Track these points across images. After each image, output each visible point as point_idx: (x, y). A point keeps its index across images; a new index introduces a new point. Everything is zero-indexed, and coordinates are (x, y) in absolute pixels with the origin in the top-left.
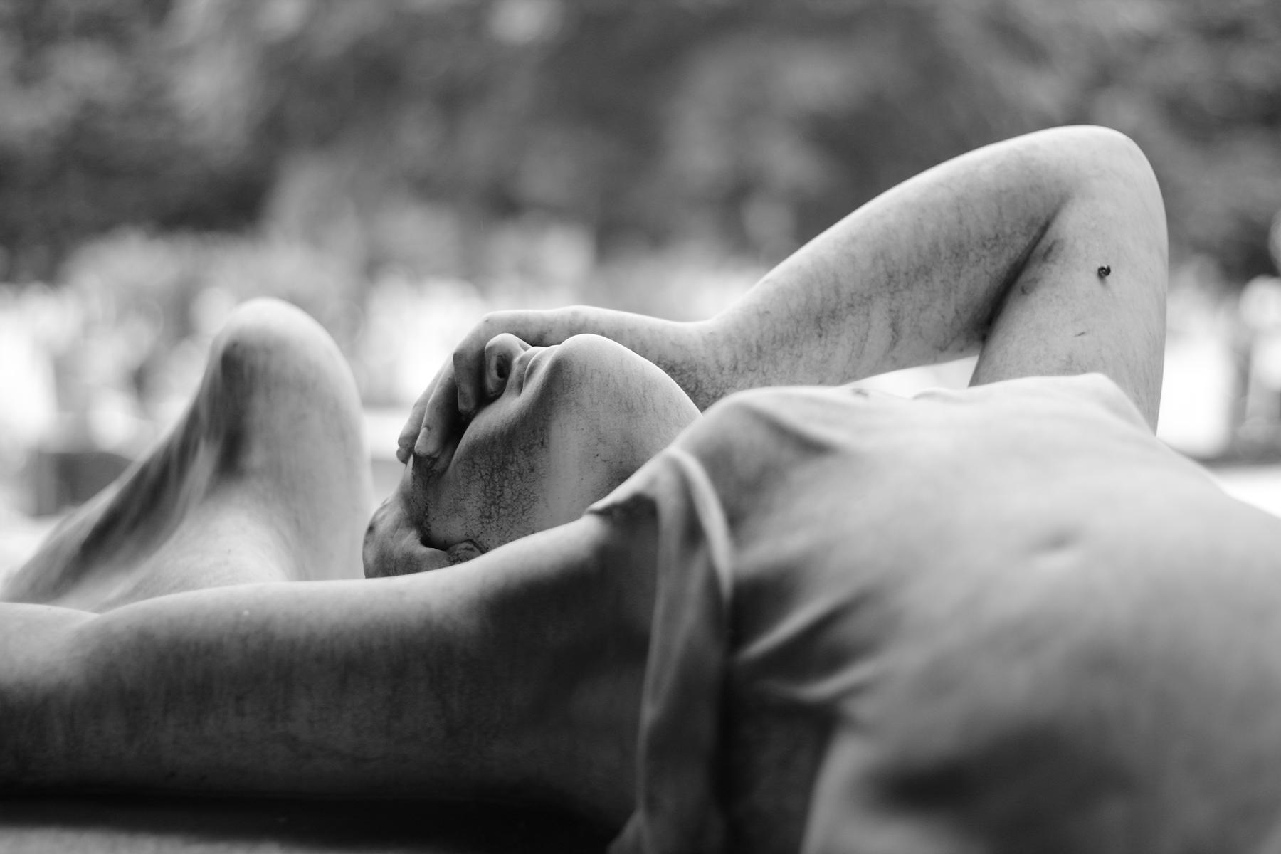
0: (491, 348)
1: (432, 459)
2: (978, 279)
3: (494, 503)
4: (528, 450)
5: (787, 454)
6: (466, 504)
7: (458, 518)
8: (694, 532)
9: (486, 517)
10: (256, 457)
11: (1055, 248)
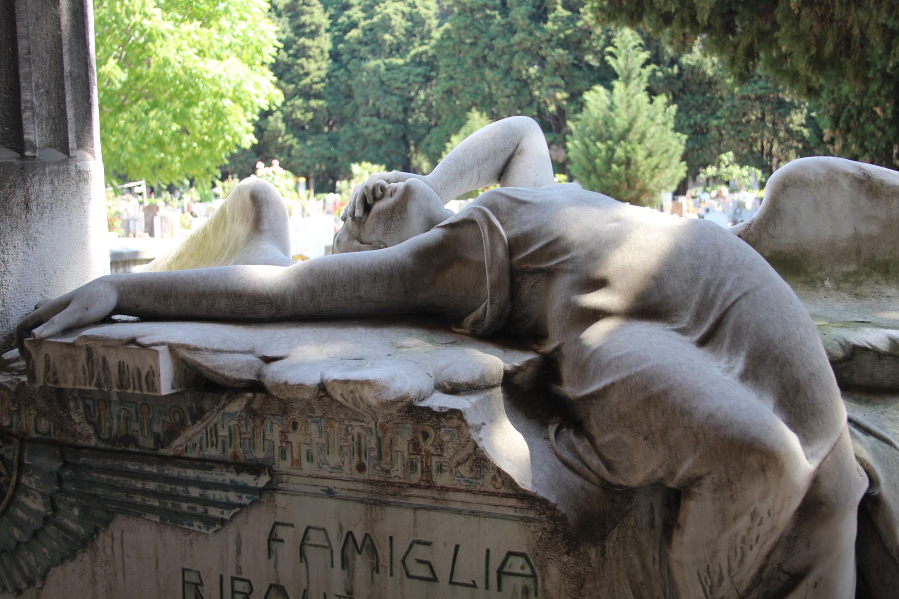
0: (378, 184)
1: (360, 218)
2: (500, 161)
4: (400, 213)
5: (514, 204)
8: (492, 227)
9: (385, 233)
10: (266, 226)
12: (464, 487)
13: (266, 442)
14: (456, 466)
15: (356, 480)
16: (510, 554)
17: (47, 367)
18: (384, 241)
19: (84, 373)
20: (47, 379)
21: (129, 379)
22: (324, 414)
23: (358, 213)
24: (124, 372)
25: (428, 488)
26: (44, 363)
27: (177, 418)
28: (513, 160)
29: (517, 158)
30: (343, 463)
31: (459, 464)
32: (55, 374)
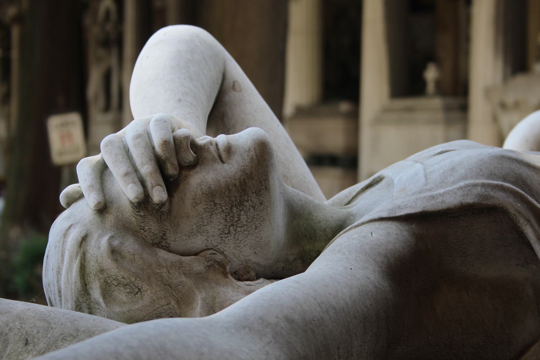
3: (233, 225)
4: (258, 193)
6: (209, 228)
7: (200, 237)
11: (236, 84)
18: (221, 247)
23: (159, 195)
28: (227, 98)
29: (232, 96)
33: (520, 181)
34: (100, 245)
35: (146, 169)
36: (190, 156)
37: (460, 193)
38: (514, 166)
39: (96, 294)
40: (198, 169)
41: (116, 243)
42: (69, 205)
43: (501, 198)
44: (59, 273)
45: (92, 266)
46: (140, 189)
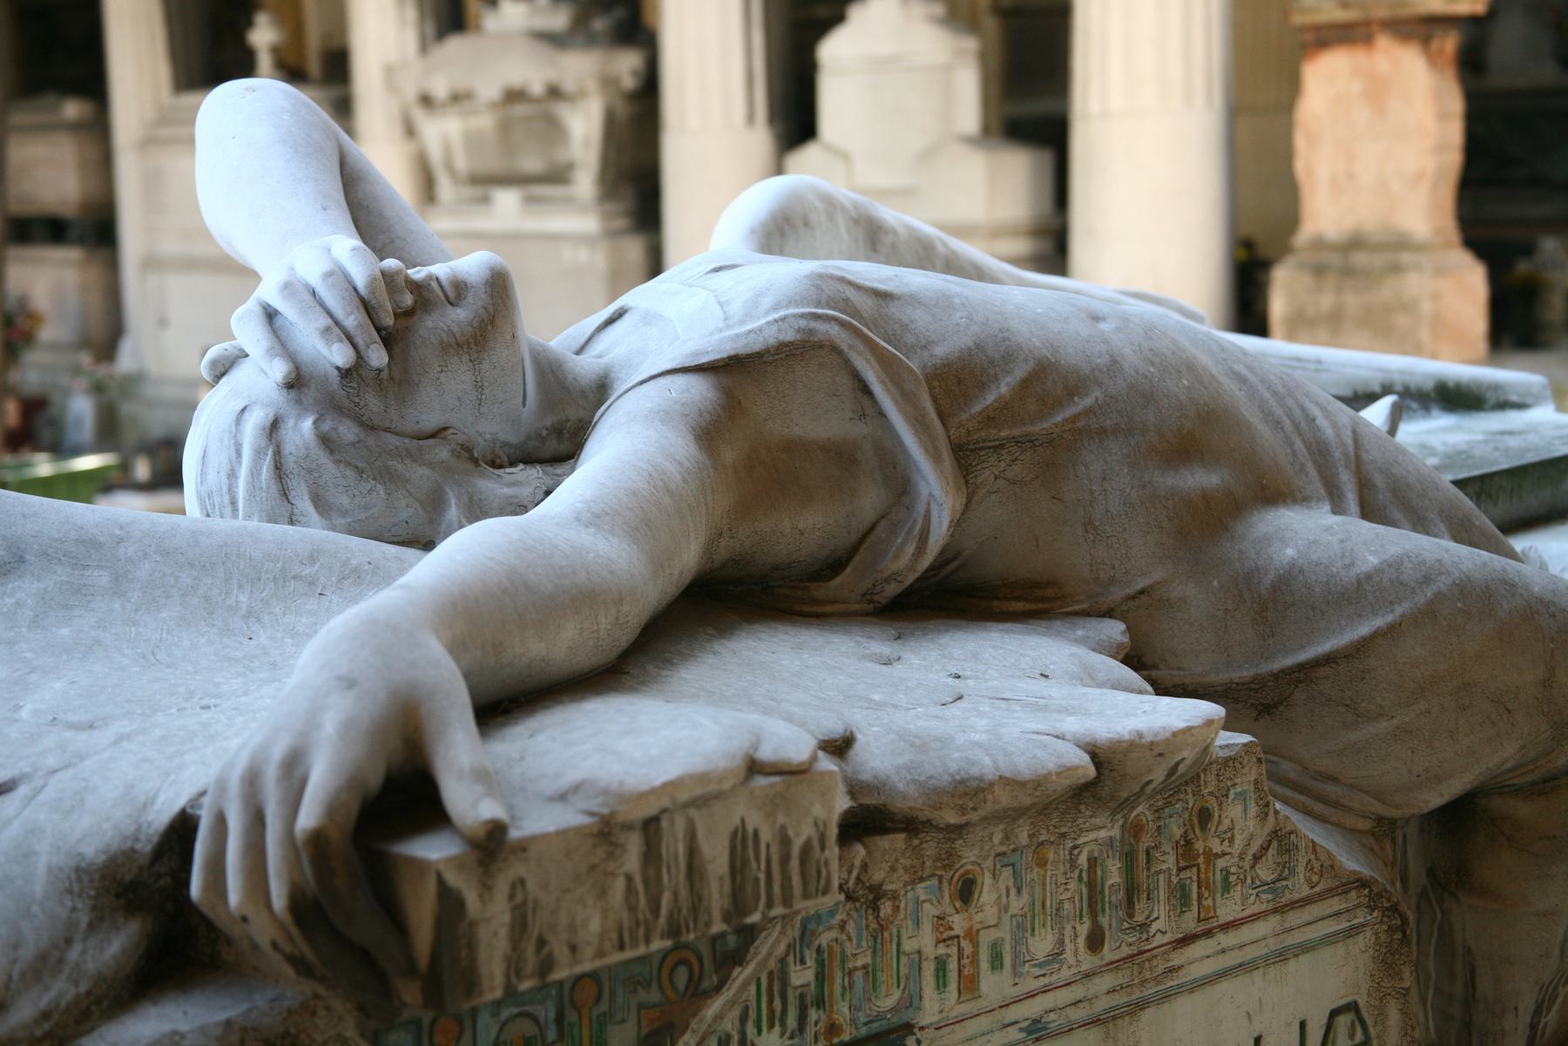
12: (1264, 907)
13: (903, 959)
14: (1252, 867)
15: (1088, 975)
16: (1334, 1014)
17: (520, 925)
19: (632, 909)
20: (514, 967)
21: (757, 880)
22: (1031, 836)
23: (378, 357)
24: (745, 862)
25: (1208, 933)
26: (506, 918)
27: (682, 976)
30: (1061, 943)
31: (1257, 858)
32: (541, 943)
33: (846, 306)
34: (302, 430)
35: (353, 320)
36: (408, 300)
37: (775, 328)
38: (839, 286)
39: (304, 504)
40: (419, 313)
41: (327, 426)
42: (219, 377)
43: (834, 331)
44: (232, 475)
45: (289, 464)
46: (350, 352)
